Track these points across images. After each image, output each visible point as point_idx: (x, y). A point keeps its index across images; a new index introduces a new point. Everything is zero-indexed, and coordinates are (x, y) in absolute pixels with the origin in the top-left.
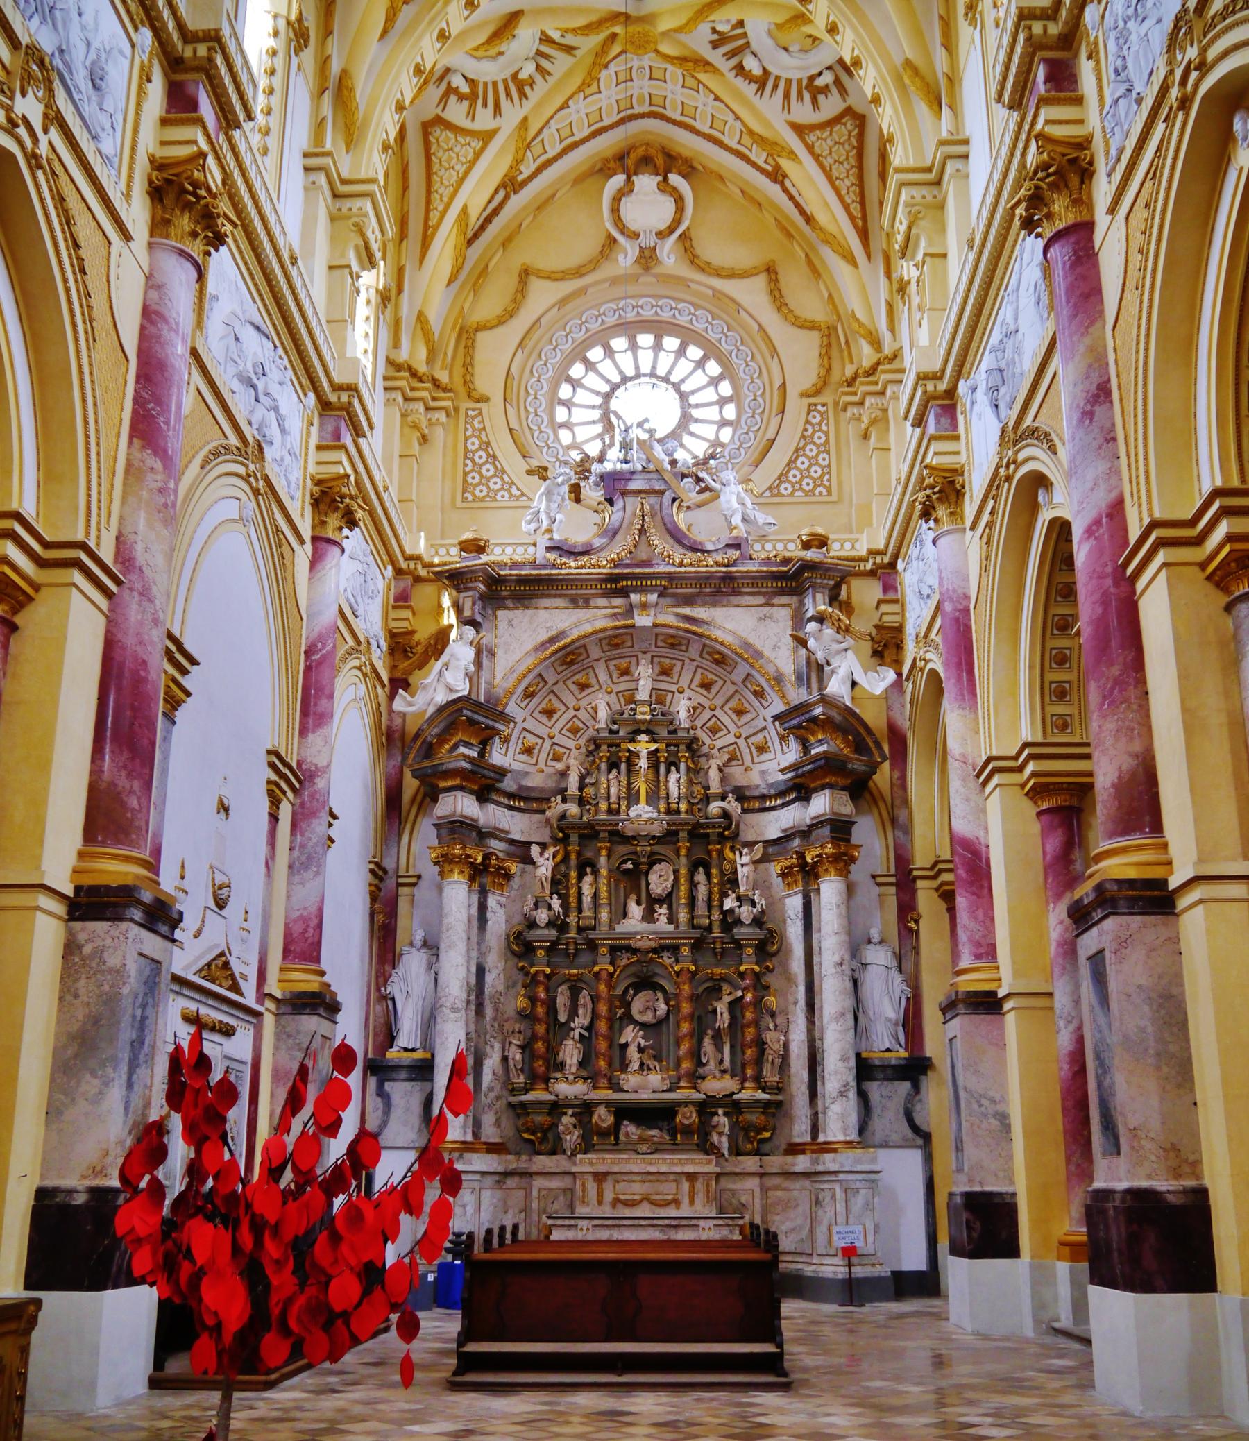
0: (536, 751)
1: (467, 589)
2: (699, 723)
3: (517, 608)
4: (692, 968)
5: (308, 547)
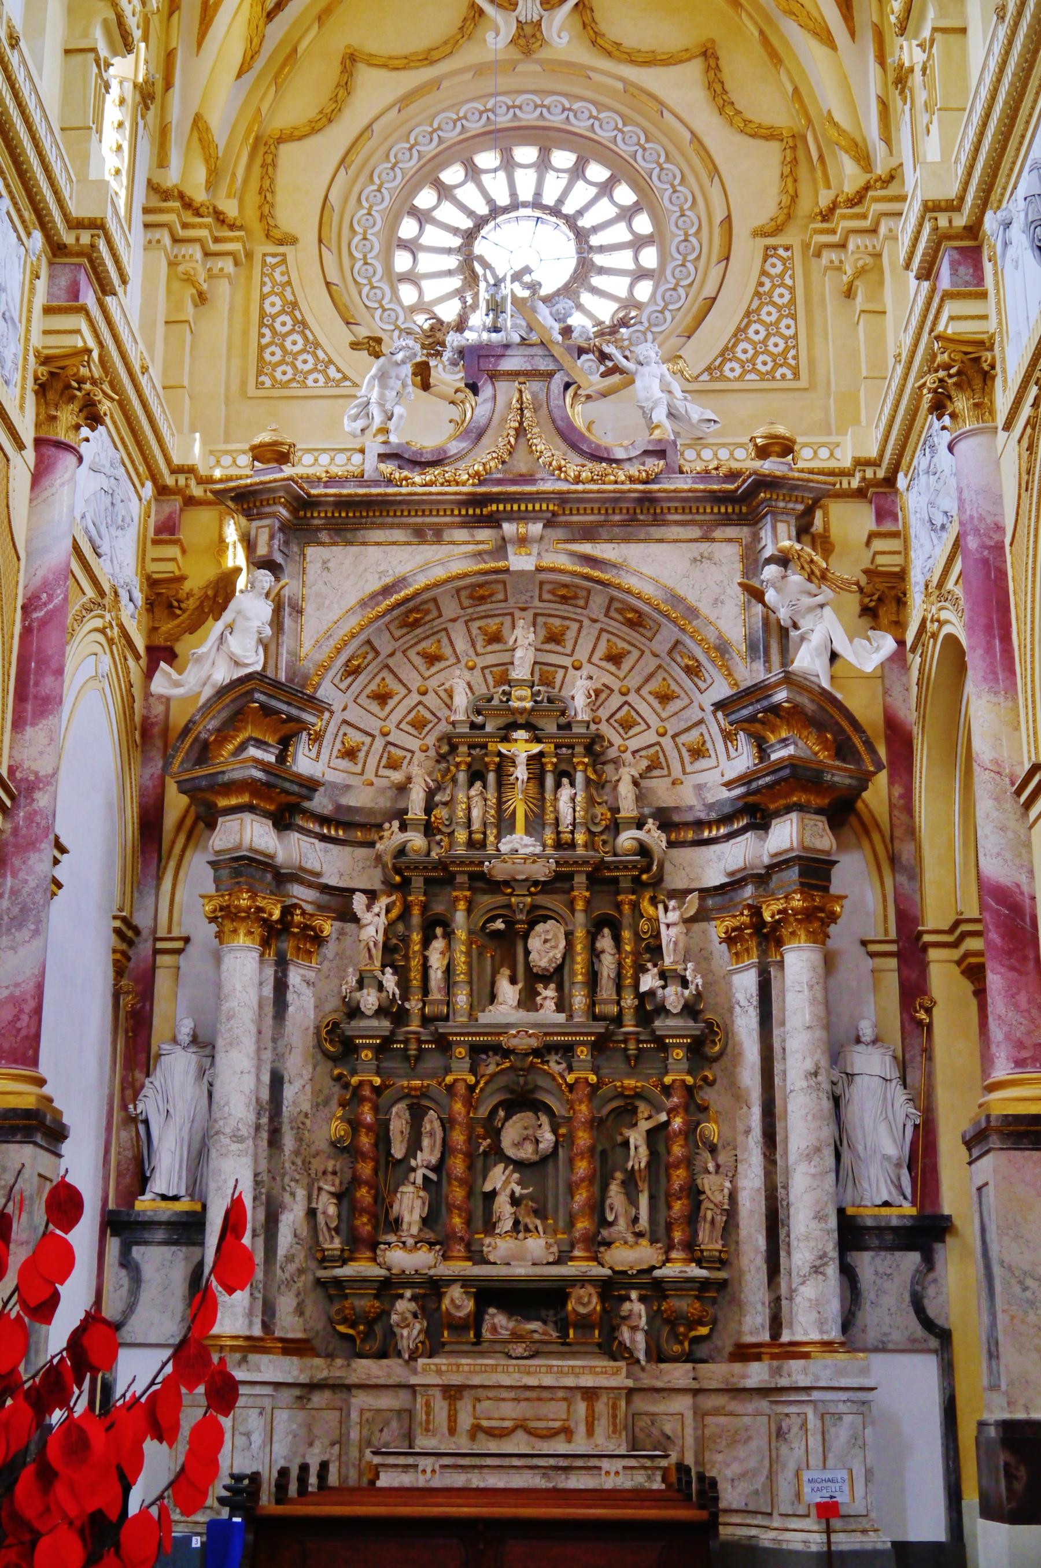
0: (361, 755)
1: (261, 516)
2: (603, 713)
3: (335, 544)
4: (593, 1078)
5: (30, 453)
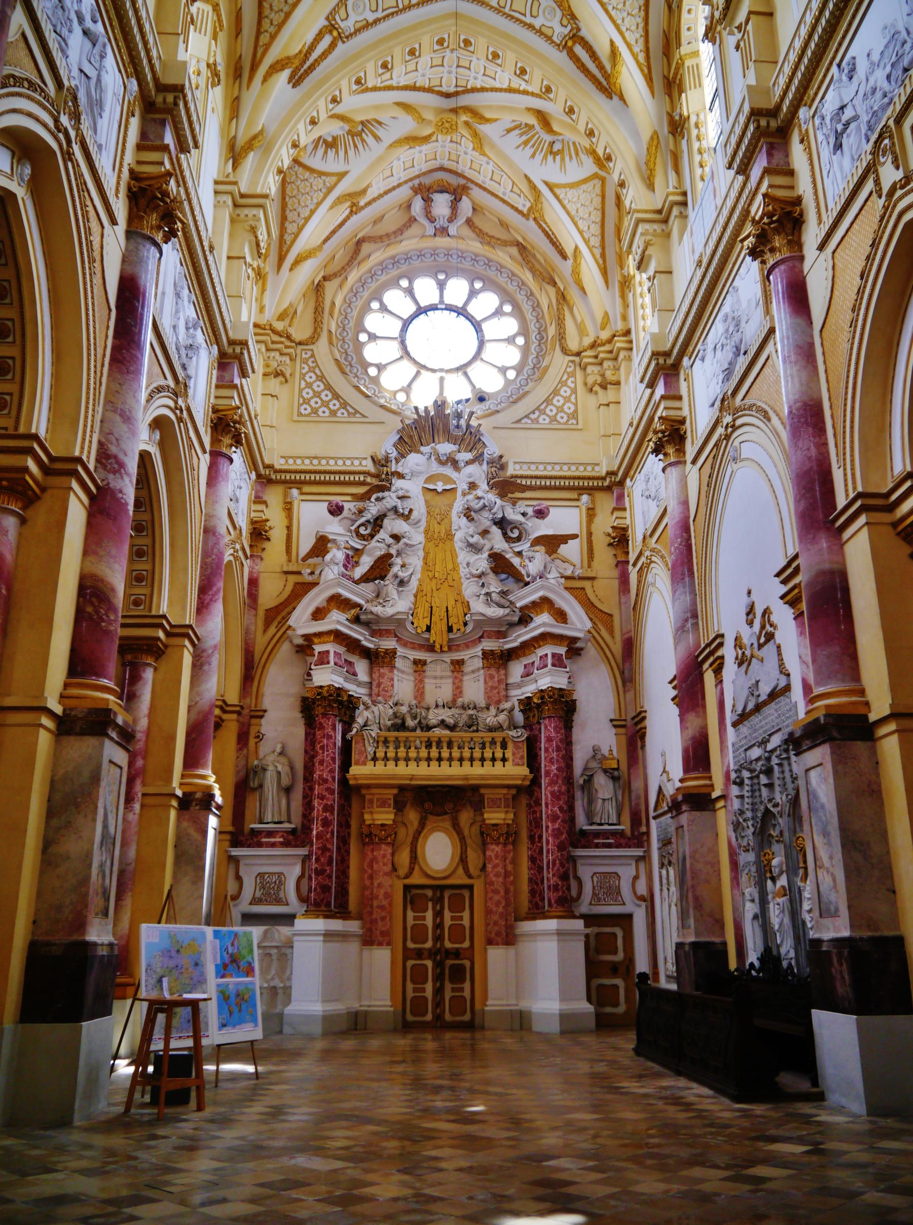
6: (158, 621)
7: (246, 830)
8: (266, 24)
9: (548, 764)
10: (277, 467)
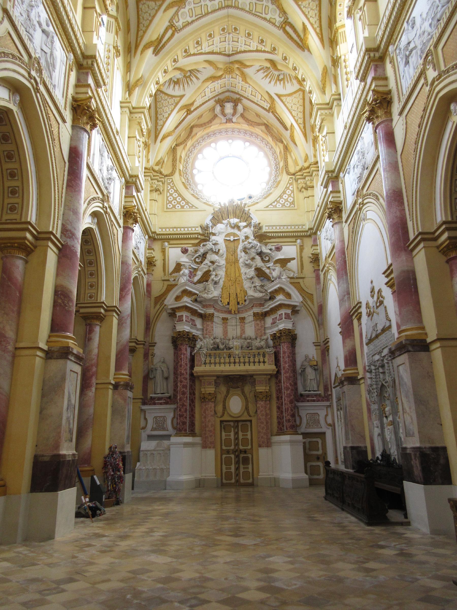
5: (122, 229)
6: (100, 305)
7: (149, 398)
8: (141, 26)
9: (285, 364)
10: (158, 232)
